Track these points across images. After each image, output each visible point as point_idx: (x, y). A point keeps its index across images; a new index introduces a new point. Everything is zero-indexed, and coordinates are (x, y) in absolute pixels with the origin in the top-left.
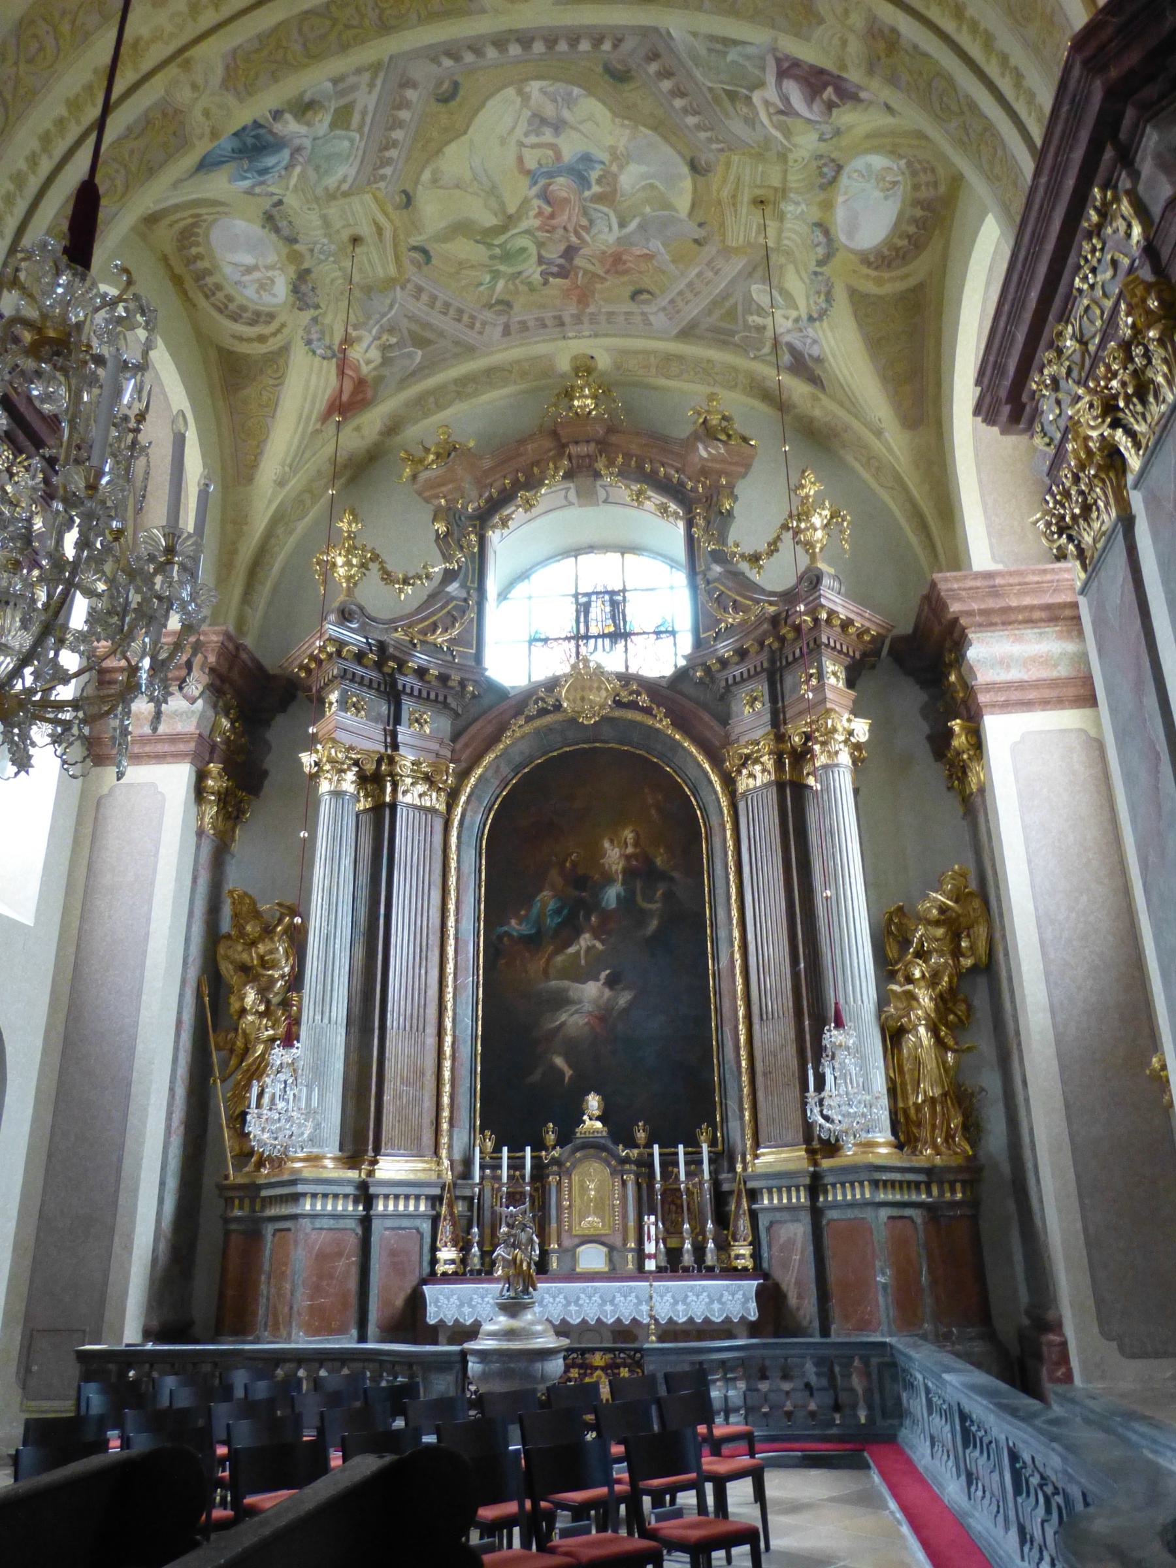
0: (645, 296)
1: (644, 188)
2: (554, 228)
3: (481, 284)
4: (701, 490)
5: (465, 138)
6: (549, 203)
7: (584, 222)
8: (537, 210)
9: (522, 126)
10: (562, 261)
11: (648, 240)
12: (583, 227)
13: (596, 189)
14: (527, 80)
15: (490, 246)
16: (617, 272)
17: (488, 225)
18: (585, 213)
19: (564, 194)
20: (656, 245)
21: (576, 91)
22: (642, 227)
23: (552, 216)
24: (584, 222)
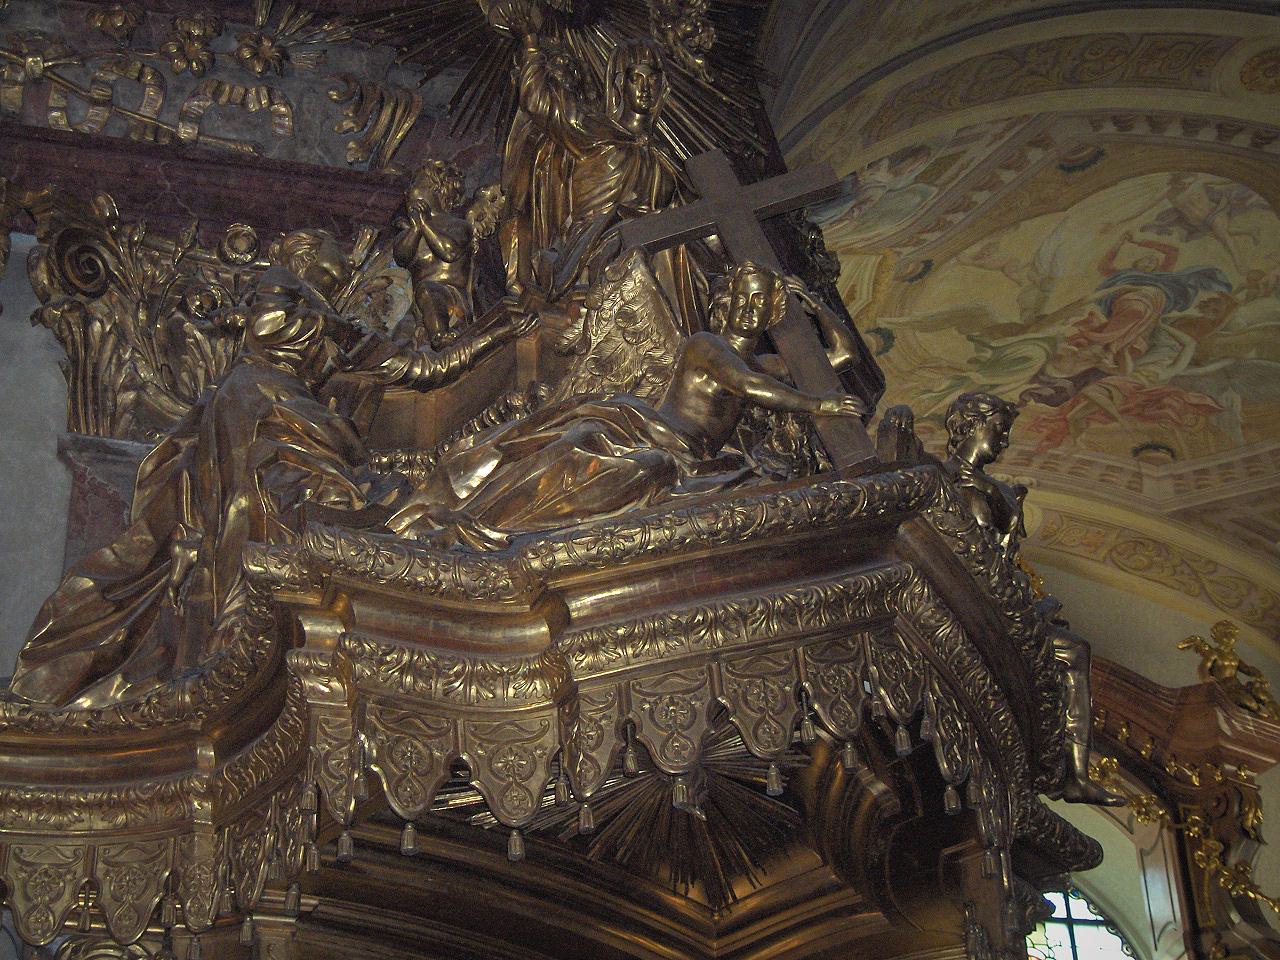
0: (1162, 454)
1: (1265, 329)
2: (1091, 343)
3: (930, 391)
4: (1196, 781)
5: (1062, 215)
6: (1109, 313)
7: (1142, 345)
8: (1086, 316)
9: (1148, 218)
10: (1068, 384)
11: (1224, 389)
12: (1134, 352)
13: (1192, 312)
14: (1196, 170)
15: (981, 345)
16: (1139, 415)
17: (1003, 320)
18: (1153, 336)
19: (1140, 307)
20: (1233, 399)
21: (1256, 198)
22: (1225, 373)
23: (1101, 329)
24: (1142, 345)
